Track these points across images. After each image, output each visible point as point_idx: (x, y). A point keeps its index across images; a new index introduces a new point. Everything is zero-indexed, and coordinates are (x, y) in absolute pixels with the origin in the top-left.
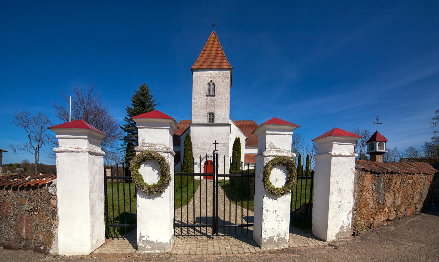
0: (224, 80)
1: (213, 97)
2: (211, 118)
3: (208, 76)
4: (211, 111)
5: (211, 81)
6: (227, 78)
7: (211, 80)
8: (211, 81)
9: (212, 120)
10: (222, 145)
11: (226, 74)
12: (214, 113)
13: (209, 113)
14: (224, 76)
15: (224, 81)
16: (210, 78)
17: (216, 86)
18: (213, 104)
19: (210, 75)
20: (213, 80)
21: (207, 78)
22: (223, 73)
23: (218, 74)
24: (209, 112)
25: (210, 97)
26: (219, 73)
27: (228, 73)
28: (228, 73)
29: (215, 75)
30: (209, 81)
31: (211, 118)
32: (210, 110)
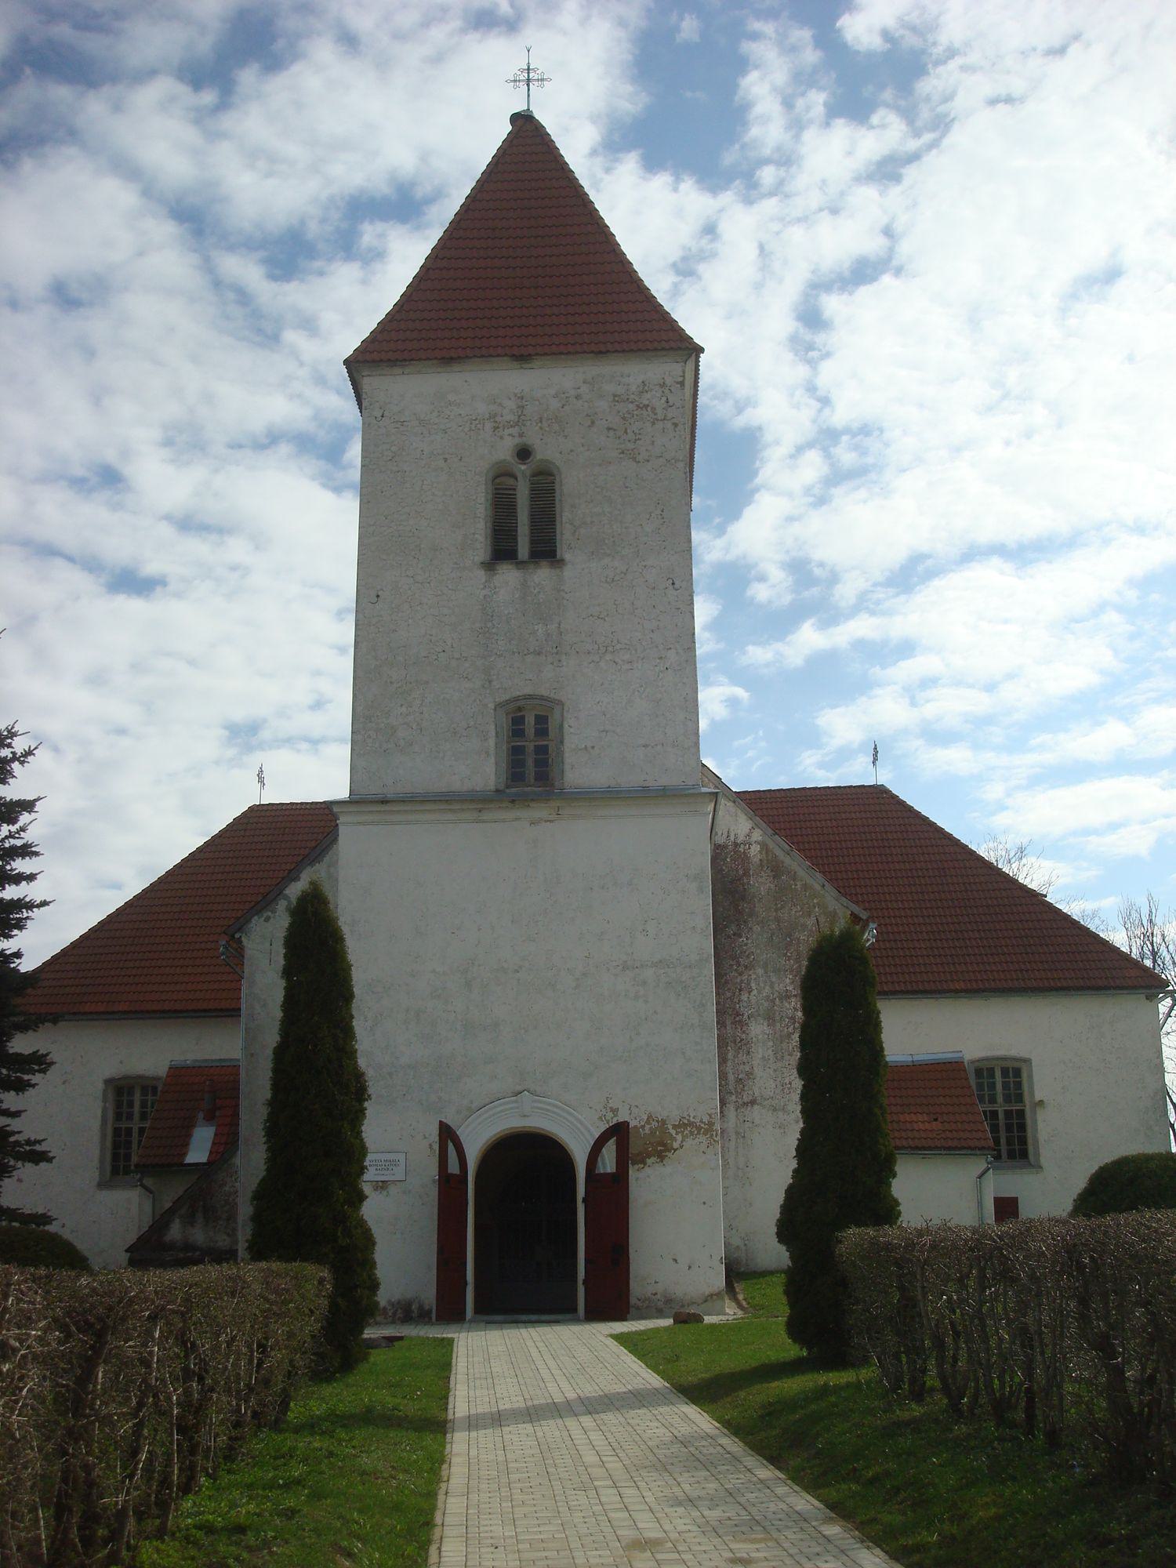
0: (631, 436)
1: (543, 575)
2: (530, 747)
3: (492, 417)
4: (528, 690)
5: (524, 453)
6: (659, 425)
7: (517, 440)
8: (524, 453)
9: (537, 763)
10: (644, 983)
11: (649, 395)
12: (561, 703)
13: (508, 702)
14: (631, 406)
15: (630, 446)
16: (515, 431)
17: (571, 484)
18: (540, 629)
19: (511, 404)
20: (533, 439)
21: (489, 425)
22: (620, 390)
23: (578, 397)
24: (507, 697)
25: (508, 575)
26: (585, 389)
27: (663, 385)
28: (663, 385)
29: (555, 404)
30: (504, 450)
31: (530, 747)
32: (518, 682)
